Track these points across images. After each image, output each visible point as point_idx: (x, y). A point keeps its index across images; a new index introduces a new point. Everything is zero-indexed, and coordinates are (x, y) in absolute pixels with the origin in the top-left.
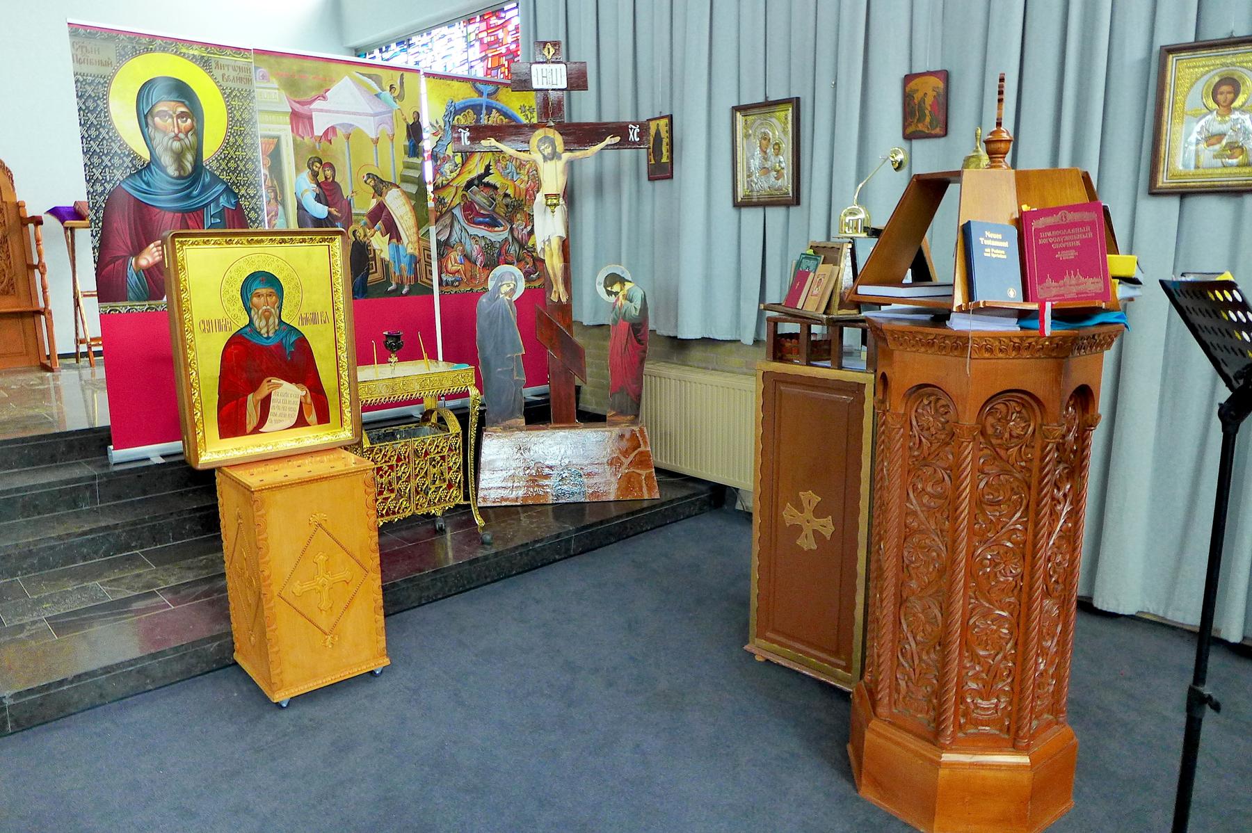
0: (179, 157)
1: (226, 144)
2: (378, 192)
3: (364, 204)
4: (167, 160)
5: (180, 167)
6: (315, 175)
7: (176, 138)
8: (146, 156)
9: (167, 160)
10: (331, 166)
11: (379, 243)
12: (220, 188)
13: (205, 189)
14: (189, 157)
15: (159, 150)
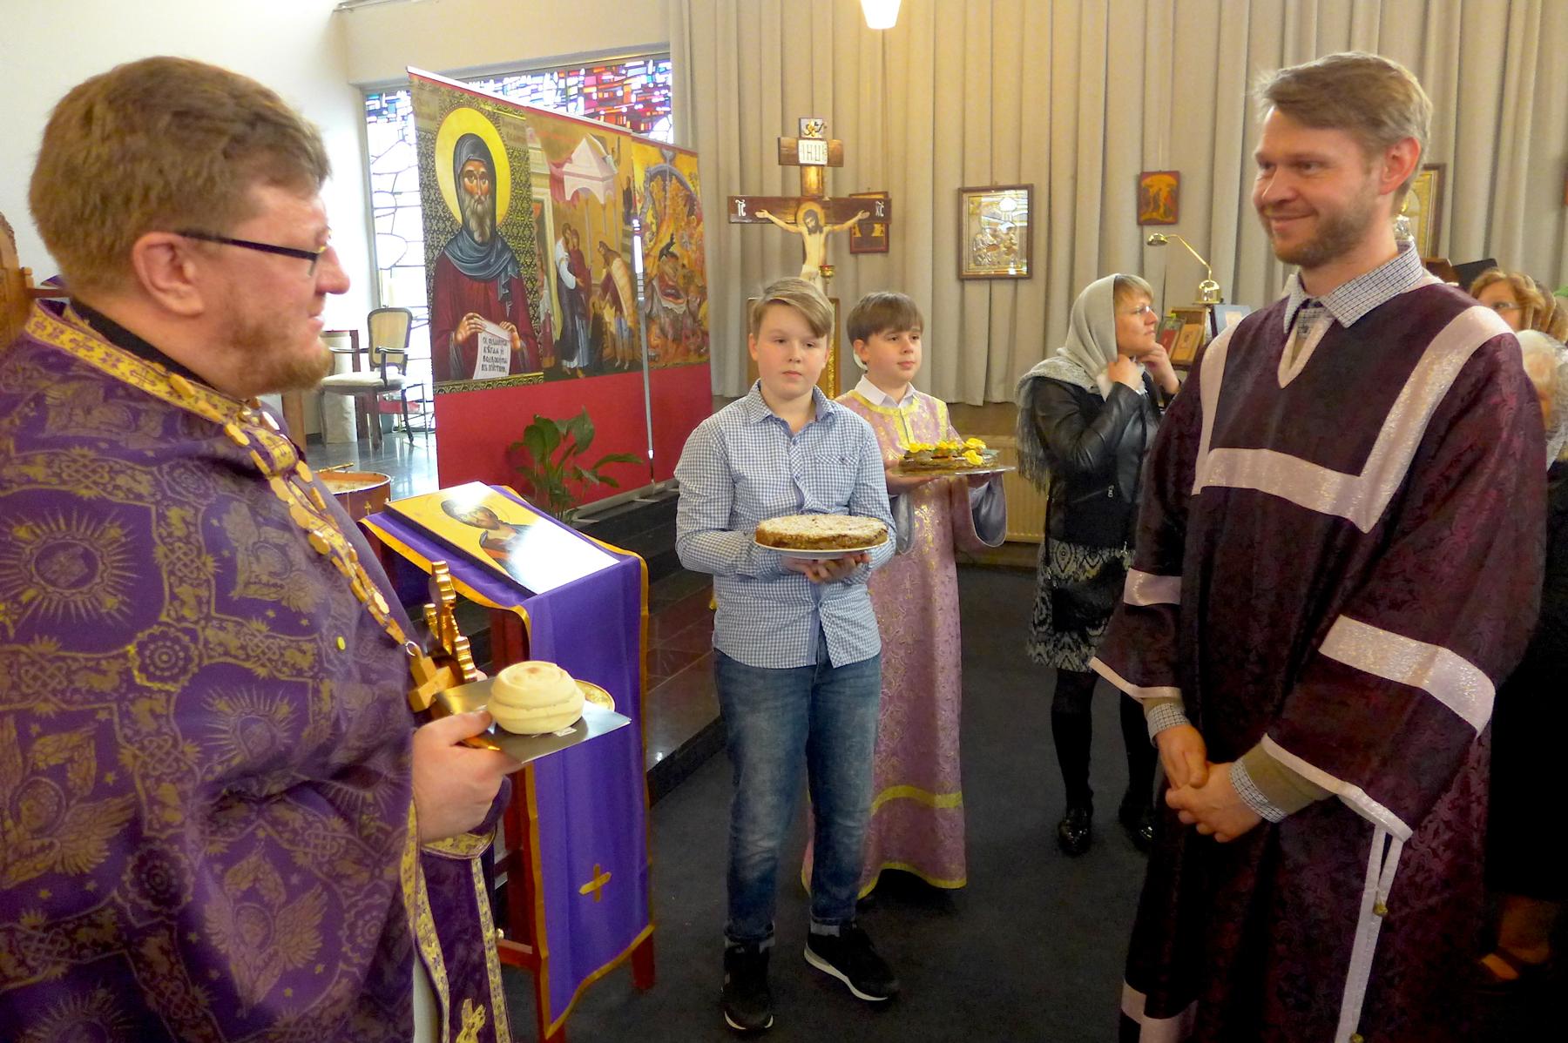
0: (481, 224)
1: (513, 210)
2: (608, 263)
3: (598, 277)
4: (473, 224)
5: (482, 234)
6: (567, 243)
7: (479, 201)
8: (459, 217)
9: (473, 224)
10: (576, 233)
11: (608, 315)
12: (507, 256)
13: (499, 256)
14: (488, 222)
15: (468, 213)
